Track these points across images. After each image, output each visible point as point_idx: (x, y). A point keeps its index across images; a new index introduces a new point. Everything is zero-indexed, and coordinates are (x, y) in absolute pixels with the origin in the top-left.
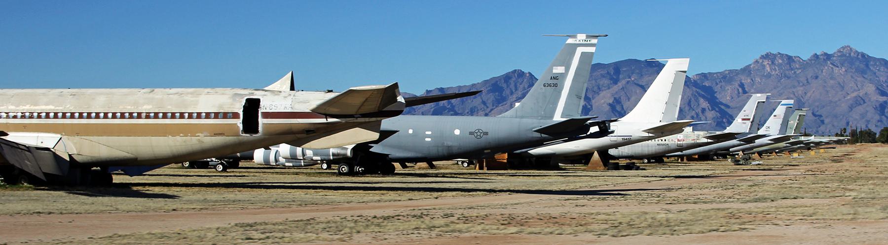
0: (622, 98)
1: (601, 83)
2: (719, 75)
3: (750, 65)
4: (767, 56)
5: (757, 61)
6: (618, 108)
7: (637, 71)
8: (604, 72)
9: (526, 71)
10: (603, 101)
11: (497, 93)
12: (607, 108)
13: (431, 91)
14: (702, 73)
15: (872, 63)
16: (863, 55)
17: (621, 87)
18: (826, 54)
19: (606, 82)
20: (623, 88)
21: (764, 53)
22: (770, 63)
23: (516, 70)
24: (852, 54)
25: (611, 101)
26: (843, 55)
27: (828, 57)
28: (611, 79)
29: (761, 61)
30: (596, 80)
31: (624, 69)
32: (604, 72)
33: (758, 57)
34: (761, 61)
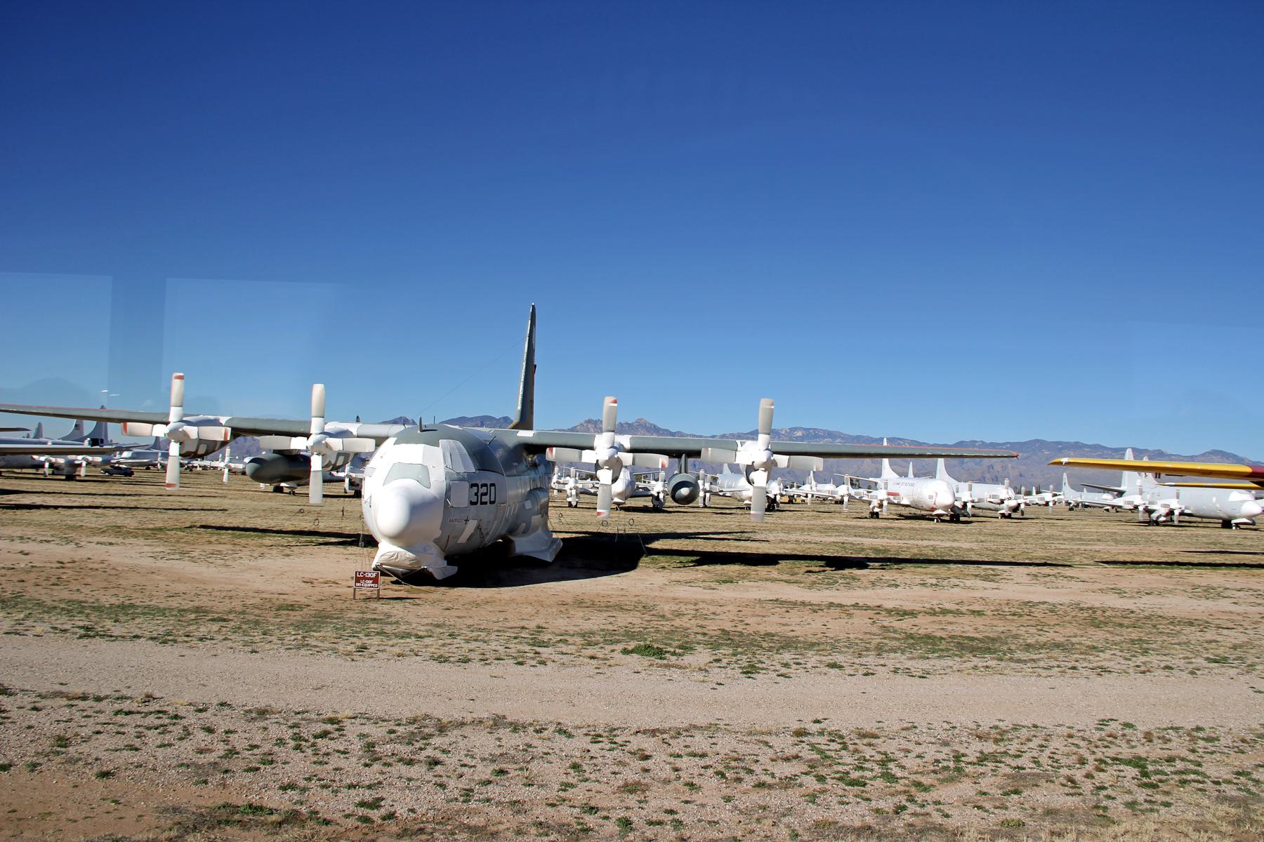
3: (576, 427)
4: (589, 421)
5: (581, 424)
15: (661, 432)
16: (655, 426)
18: (627, 423)
21: (587, 419)
22: (593, 426)
23: (401, 417)
24: (647, 425)
26: (641, 425)
27: (629, 425)
29: (585, 425)
33: (582, 421)
34: (585, 425)
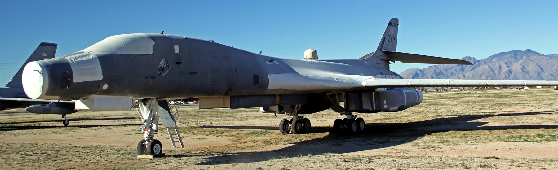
0: (525, 66)
1: (511, 60)
2: (557, 55)
6: (525, 70)
7: (525, 54)
8: (510, 55)
9: (471, 56)
10: (516, 67)
11: (461, 66)
12: (521, 70)
13: (431, 66)
14: (548, 55)
17: (523, 61)
19: (513, 59)
20: (524, 62)
23: (467, 56)
25: (521, 67)
28: (514, 58)
30: (508, 59)
31: (519, 54)
32: (510, 55)
